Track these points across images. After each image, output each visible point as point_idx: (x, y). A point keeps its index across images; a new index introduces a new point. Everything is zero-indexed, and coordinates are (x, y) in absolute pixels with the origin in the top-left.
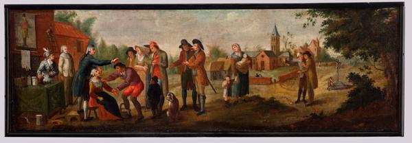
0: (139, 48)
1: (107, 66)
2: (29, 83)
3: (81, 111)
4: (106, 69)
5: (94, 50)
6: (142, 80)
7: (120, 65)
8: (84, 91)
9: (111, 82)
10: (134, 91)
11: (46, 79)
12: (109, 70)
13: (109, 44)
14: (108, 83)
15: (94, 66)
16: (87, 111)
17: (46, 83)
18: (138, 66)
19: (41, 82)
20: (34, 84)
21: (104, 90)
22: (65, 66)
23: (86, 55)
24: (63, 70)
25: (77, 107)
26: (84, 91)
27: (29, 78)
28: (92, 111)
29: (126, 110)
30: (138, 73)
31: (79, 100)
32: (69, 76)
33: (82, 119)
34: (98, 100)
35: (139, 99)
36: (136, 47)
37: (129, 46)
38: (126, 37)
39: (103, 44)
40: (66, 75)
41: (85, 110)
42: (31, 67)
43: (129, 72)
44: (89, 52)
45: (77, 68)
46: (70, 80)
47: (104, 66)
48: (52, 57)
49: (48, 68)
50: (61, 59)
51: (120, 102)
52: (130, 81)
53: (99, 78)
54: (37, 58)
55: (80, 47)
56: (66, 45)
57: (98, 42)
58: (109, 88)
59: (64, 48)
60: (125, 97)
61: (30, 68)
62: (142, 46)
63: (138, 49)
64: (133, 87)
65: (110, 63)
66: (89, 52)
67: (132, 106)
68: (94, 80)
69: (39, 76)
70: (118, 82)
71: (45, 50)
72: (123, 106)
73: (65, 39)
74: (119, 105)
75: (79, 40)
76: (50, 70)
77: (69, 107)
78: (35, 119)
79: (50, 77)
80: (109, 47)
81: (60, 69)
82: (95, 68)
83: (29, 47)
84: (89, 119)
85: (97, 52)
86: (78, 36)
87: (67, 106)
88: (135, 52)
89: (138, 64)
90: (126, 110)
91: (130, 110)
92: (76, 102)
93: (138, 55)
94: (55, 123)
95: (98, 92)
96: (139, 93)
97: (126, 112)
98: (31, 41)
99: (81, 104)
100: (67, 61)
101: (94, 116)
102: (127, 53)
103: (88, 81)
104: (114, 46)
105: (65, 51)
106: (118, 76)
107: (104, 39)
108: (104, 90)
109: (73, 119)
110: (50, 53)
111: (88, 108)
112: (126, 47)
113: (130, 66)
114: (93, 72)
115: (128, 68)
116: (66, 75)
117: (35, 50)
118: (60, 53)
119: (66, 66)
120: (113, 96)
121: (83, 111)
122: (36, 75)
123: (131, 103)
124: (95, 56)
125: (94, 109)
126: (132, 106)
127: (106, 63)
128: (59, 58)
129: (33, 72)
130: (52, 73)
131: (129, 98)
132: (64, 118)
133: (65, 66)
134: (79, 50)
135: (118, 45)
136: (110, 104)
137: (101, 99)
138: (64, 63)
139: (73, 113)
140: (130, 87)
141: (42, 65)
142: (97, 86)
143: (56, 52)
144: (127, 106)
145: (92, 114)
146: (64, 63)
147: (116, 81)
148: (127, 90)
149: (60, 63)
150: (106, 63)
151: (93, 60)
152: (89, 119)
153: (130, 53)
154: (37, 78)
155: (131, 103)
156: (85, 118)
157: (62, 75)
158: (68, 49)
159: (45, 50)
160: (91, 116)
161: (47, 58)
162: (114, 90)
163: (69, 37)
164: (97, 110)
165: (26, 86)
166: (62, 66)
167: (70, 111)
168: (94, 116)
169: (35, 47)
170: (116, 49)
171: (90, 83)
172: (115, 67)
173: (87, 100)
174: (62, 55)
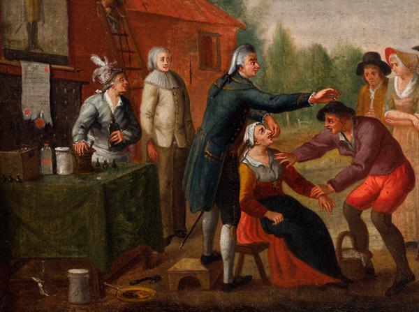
0: (401, 55)
1: (297, 112)
2: (47, 167)
3: (212, 259)
4: (293, 121)
5: (253, 60)
6: (408, 158)
7: (339, 109)
8: (223, 193)
9: (310, 165)
10: (383, 194)
11: (101, 154)
12: (302, 127)
13: (301, 42)
14: (298, 166)
15: (253, 112)
16: (231, 258)
17: (99, 168)
18: (393, 114)
19: (83, 164)
20: (62, 170)
21: (287, 190)
22: (160, 114)
23: (229, 79)
24: (154, 126)
25: (199, 244)
26: (223, 193)
27: (46, 151)
28: (249, 258)
29: (356, 255)
30: (396, 135)
31: (206, 221)
32: (173, 146)
33: (217, 284)
34: (267, 223)
35: (398, 219)
36: (389, 51)
37: (365, 49)
38: (355, 20)
39: (283, 42)
40: (164, 140)
41: (224, 253)
42: (53, 113)
43: (367, 134)
44: (238, 67)
45: (198, 118)
46: (179, 157)
47: (287, 114)
48: (119, 86)
49: (107, 119)
50: (147, 91)
51: (337, 228)
52: (370, 162)
53: (270, 151)
54: (71, 86)
55: (208, 51)
56: (162, 44)
57: (268, 35)
58: (303, 185)
59: (158, 56)
60: (353, 214)
61: (49, 120)
62: (407, 47)
63: (395, 58)
64: (379, 181)
65: (306, 104)
66: (238, 67)
67: (376, 242)
68: (254, 159)
69: (79, 145)
70: (333, 163)
71: (97, 60)
72: (348, 242)
73: (161, 28)
74: (334, 236)
75: (206, 29)
76: (114, 127)
77: (174, 245)
78: (64, 284)
79: (114, 146)
80: (303, 53)
81: (145, 122)
82: (258, 119)
83: (47, 51)
84: (239, 282)
85: (262, 68)
86: (202, 19)
87: (168, 241)
88: (385, 69)
89: (394, 108)
90: (356, 255)
91: (370, 255)
92: (197, 229)
93: (395, 78)
94: (130, 295)
95: (267, 196)
96: (397, 200)
97: (359, 261)
98: (53, 34)
99: (213, 233)
100: (168, 97)
101: (256, 275)
102: (360, 71)
103: (234, 161)
104: (319, 51)
105: (161, 65)
106: (331, 144)
107: (287, 25)
108: (287, 190)
109: (189, 281)
110: (114, 72)
111: (235, 247)
112: (355, 54)
113: (369, 114)
114: (252, 131)
115: (362, 119)
116: (164, 140)
117: (64, 60)
118: (146, 72)
119: (166, 113)
120: (316, 210)
121: (219, 257)
122: (67, 141)
123: (373, 231)
124: (256, 82)
125: (254, 249)
126: (376, 242)
127: (294, 103)
128: (140, 88)
129: (58, 133)
130: (118, 136)
131: (366, 215)
132: (157, 279)
133: (160, 114)
134: (207, 61)
135: (330, 48)
136: (306, 234)
137: (276, 218)
138: (157, 101)
139: (189, 264)
140: (369, 181)
141: (86, 110)
142: (264, 176)
143: (132, 69)
144: (359, 234)
145: (250, 269)
146: (157, 101)
147: (323, 162)
148: (360, 191)
149: (146, 105)
150: (294, 103)
151: (252, 94)
152: (239, 282)
153: (368, 70)
154: (72, 151)
155: (373, 231)
156: (226, 280)
157: (153, 142)
158: (170, 59)
159: (97, 60)
160: (245, 273)
161: (103, 87)
162: (317, 190)
163: (177, 20)
164: (263, 255)
165: (37, 177)
166: (153, 115)
167: (177, 255)
168: (256, 275)
169: (65, 51)
170: (326, 56)
171: (243, 169)
172: (321, 117)
173: (234, 221)
174: (153, 78)
